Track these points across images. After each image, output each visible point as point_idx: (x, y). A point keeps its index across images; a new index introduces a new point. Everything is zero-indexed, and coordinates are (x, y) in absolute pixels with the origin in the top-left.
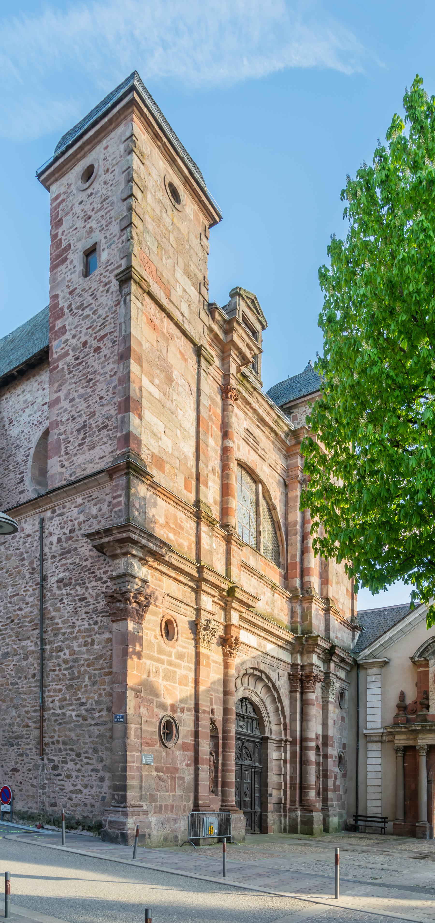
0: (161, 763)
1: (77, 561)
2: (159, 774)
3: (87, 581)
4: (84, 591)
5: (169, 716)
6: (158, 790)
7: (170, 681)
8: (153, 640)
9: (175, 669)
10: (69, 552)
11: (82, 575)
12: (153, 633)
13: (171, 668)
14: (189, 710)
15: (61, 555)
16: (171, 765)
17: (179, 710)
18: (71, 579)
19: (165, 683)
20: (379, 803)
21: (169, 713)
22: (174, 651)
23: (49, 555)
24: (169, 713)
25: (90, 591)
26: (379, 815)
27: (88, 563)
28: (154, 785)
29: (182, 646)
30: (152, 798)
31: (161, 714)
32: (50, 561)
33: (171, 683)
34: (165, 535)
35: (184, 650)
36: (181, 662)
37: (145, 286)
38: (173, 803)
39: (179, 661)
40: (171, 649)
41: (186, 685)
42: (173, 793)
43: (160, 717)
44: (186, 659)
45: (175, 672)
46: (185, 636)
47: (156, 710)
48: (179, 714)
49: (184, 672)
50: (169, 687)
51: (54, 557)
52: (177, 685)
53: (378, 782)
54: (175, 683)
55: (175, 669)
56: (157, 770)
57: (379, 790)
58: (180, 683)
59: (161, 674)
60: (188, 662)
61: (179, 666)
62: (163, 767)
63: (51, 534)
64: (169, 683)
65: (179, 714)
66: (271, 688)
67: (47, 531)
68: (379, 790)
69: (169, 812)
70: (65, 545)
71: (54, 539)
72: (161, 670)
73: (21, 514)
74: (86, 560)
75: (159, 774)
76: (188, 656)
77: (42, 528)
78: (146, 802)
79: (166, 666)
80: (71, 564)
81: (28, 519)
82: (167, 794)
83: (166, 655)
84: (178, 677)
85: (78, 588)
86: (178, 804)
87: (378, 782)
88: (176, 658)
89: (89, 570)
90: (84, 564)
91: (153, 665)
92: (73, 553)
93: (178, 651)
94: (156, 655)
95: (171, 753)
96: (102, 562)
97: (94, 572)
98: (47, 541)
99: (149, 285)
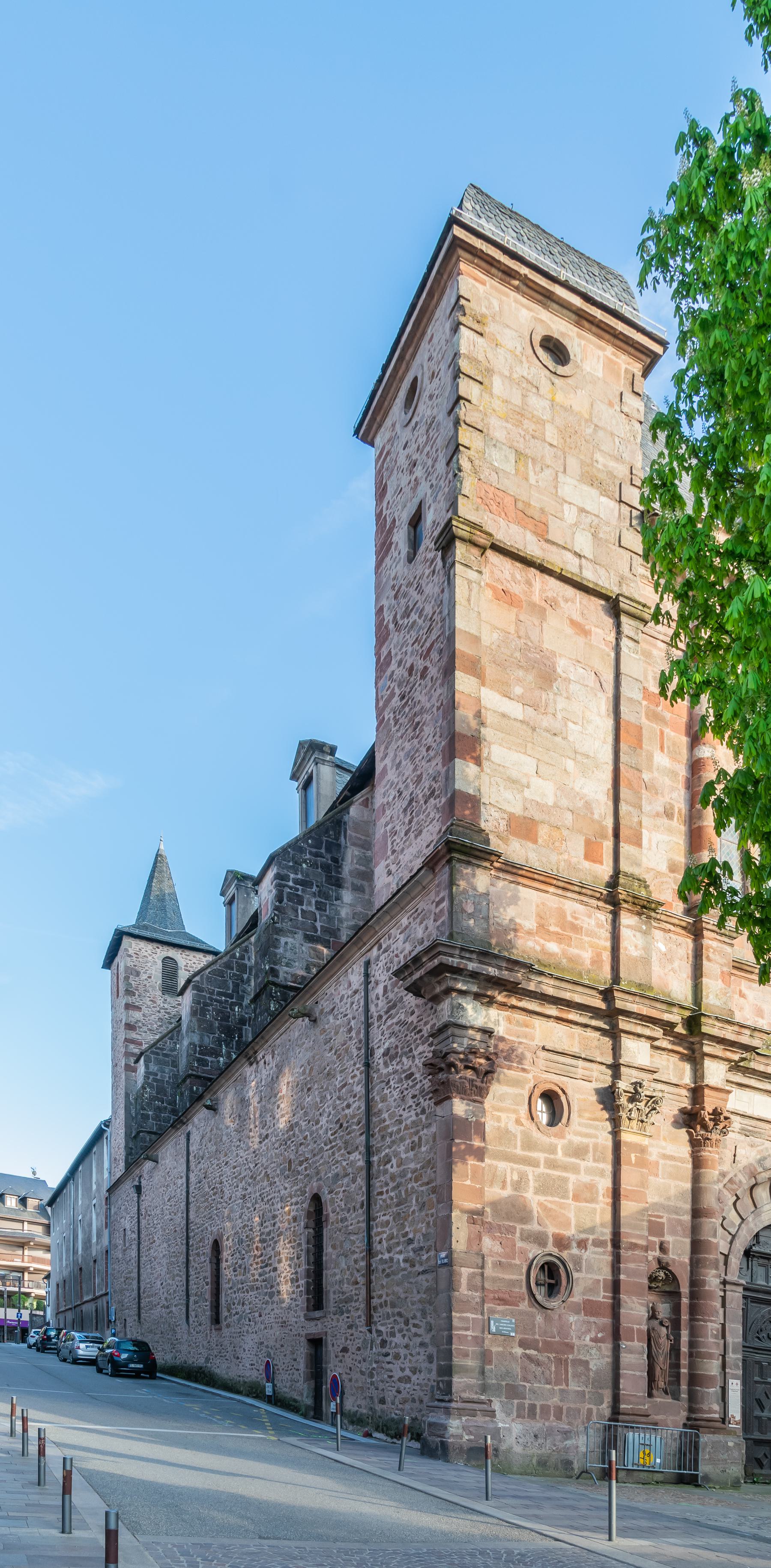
1: (403, 1017)
2: (528, 1352)
3: (413, 1046)
4: (410, 1062)
5: (551, 1255)
6: (525, 1379)
7: (552, 1195)
8: (512, 1127)
10: (394, 1006)
11: (408, 1038)
15: (387, 1012)
18: (397, 1047)
19: (542, 1198)
21: (551, 1248)
23: (375, 1015)
24: (551, 1248)
25: (417, 1061)
27: (413, 1019)
28: (517, 1370)
30: (513, 1392)
31: (533, 1251)
32: (376, 1025)
33: (557, 1199)
37: (482, 540)
43: (531, 1256)
47: (520, 1244)
50: (549, 1205)
51: (380, 1017)
63: (377, 983)
64: (550, 1198)
67: (373, 979)
70: (391, 995)
71: (380, 990)
72: (531, 1177)
73: (347, 961)
74: (413, 1013)
75: (528, 1352)
77: (367, 975)
78: (499, 1396)
79: (542, 1169)
80: (397, 1024)
81: (354, 967)
83: (543, 1150)
85: (404, 1059)
89: (415, 1027)
90: (410, 1020)
91: (512, 1170)
92: (399, 1005)
94: (519, 1151)
96: (429, 1011)
97: (420, 1031)
98: (372, 995)
99: (490, 535)
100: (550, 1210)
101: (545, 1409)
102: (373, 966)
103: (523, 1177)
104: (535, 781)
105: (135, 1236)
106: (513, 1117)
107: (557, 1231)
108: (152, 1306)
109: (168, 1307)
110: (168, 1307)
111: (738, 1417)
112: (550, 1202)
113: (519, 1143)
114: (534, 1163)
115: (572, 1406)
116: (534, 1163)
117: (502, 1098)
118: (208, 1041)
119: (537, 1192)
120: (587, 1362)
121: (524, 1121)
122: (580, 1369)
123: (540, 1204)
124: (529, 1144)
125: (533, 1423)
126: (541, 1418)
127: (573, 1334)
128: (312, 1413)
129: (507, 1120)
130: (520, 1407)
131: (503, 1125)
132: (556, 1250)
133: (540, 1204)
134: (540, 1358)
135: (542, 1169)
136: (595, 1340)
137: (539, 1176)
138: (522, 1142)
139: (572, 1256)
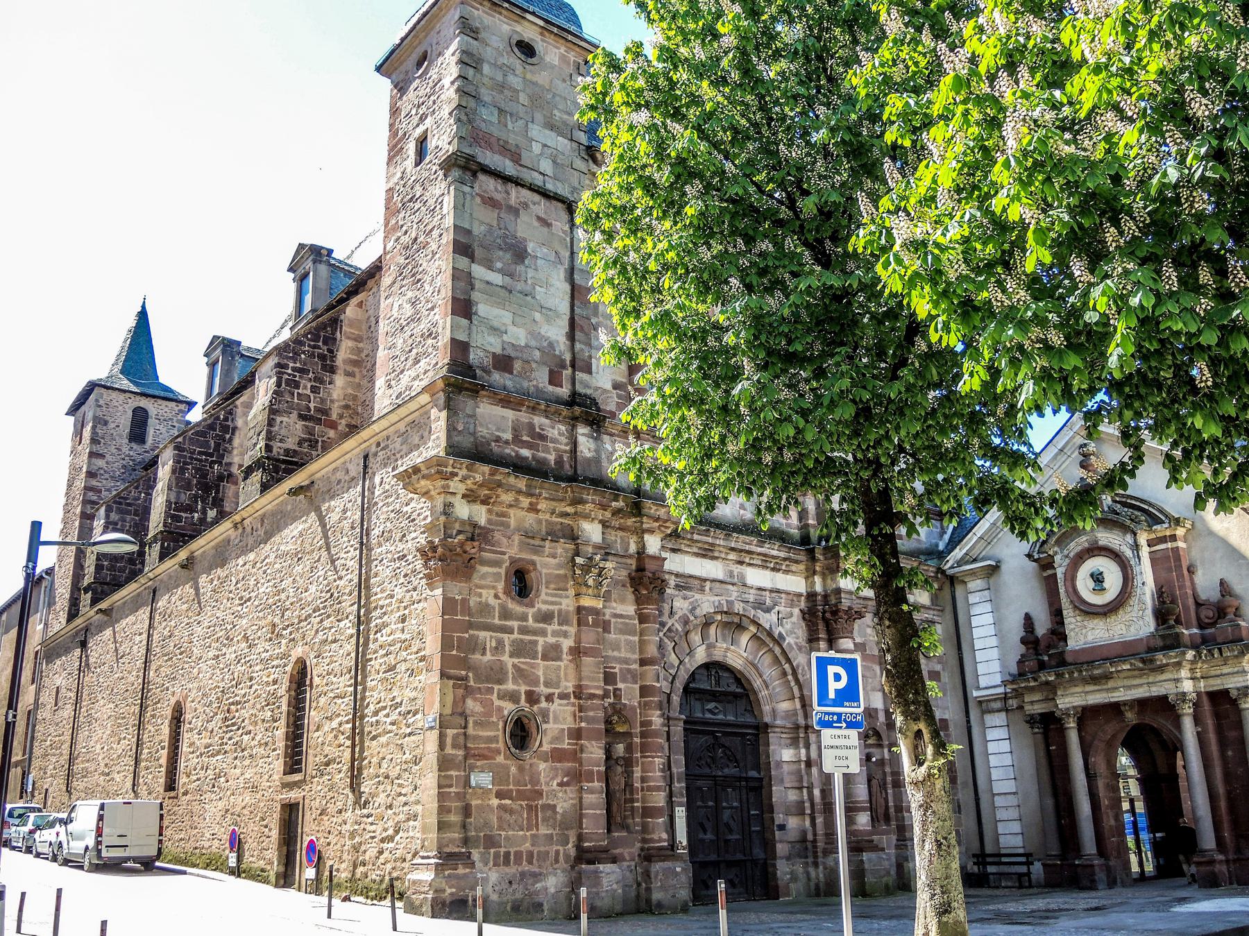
8: (492, 601)
12: (492, 592)
17: (543, 699)
19: (516, 660)
20: (1016, 827)
26: (1021, 851)
35: (551, 607)
45: (536, 642)
49: (551, 640)
50: (523, 666)
53: (1010, 786)
54: (535, 658)
57: (1013, 801)
59: (507, 649)
61: (543, 633)
65: (544, 704)
66: (767, 639)
68: (1013, 801)
84: (540, 649)
87: (1010, 786)
94: (497, 621)
100: (523, 670)
101: (518, 855)
102: (371, 459)
103: (500, 643)
104: (512, 329)
105: (73, 695)
108: (86, 774)
109: (108, 774)
110: (108, 774)
111: (685, 843)
114: (509, 631)
115: (542, 849)
116: (509, 631)
118: (185, 498)
120: (555, 806)
122: (549, 813)
123: (514, 666)
125: (507, 870)
126: (515, 863)
127: (542, 780)
128: (282, 882)
130: (497, 855)
131: (483, 600)
133: (514, 666)
135: (516, 636)
136: (561, 784)
139: (541, 709)
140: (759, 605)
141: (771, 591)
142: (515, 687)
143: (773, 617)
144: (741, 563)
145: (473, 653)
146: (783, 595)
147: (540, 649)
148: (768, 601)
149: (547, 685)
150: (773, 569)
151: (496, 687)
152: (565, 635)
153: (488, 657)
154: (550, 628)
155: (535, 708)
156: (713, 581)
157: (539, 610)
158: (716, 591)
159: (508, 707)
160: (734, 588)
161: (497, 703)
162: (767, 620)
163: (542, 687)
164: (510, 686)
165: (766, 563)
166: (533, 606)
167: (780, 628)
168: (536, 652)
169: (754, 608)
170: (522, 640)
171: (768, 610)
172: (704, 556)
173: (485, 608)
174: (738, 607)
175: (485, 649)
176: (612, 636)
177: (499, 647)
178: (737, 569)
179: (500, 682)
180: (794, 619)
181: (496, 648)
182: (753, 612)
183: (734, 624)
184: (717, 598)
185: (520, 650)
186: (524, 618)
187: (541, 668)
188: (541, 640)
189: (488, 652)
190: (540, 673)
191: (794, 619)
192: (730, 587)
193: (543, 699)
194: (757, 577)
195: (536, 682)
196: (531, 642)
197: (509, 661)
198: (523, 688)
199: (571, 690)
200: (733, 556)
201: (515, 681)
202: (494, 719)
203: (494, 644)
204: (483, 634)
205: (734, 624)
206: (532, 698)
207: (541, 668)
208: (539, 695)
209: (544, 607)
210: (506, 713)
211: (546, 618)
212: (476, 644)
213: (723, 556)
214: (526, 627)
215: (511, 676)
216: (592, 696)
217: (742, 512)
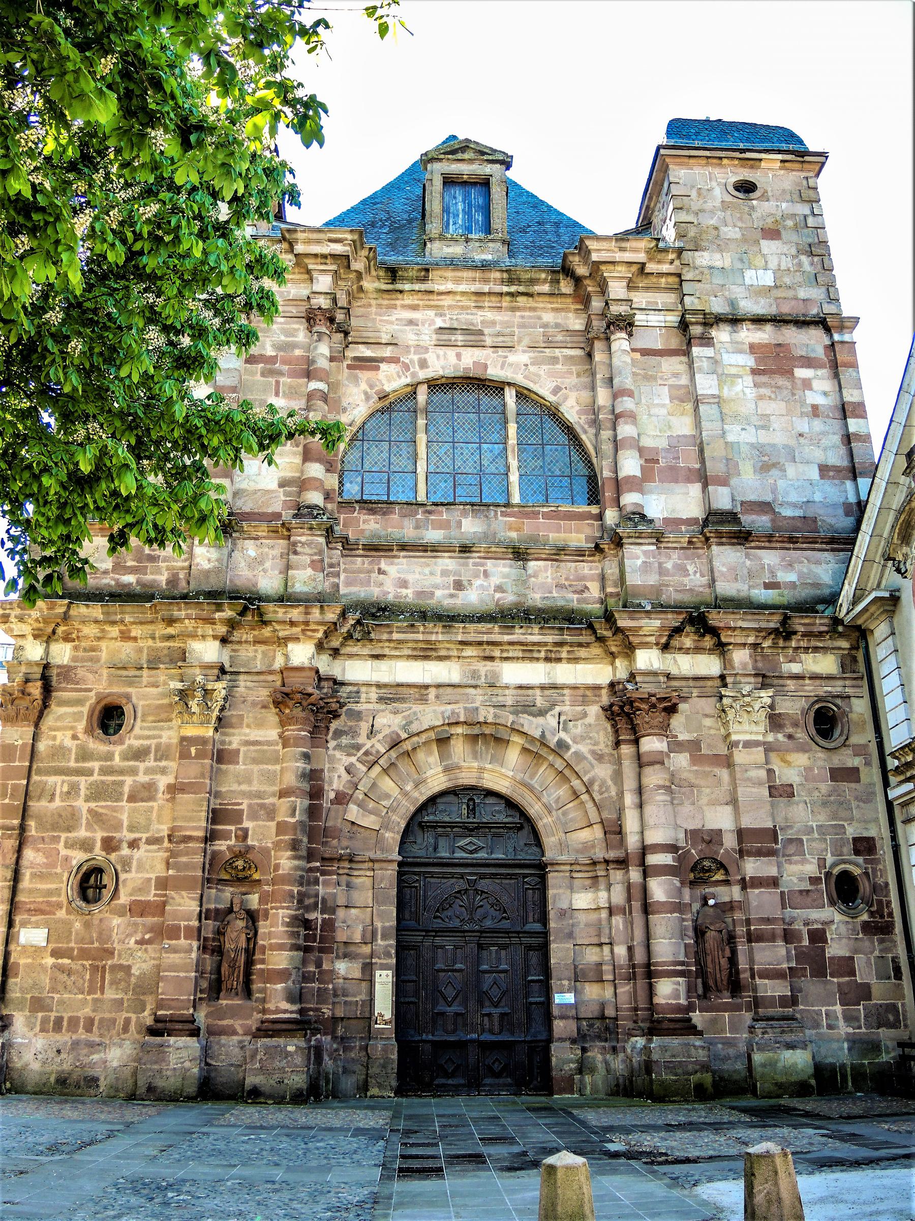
0: (70, 941)
7: (105, 800)
9: (120, 778)
13: (110, 778)
14: (149, 842)
16: (96, 945)
17: (125, 845)
22: (118, 750)
29: (138, 738)
34: (113, 583)
36: (137, 763)
38: (92, 1015)
39: (131, 763)
40: (111, 748)
41: (151, 798)
42: (98, 995)
44: (152, 756)
46: (151, 718)
48: (125, 851)
49: (142, 778)
50: (100, 810)
52: (124, 803)
55: (120, 778)
56: (55, 954)
58: (132, 798)
59: (83, 792)
60: (156, 760)
61: (133, 772)
62: (72, 949)
64: (103, 804)
65: (125, 851)
69: (81, 1030)
76: (156, 751)
82: (80, 996)
84: (126, 789)
86: (107, 1015)
88: (125, 757)
93: (130, 746)
95: (96, 922)
100: (101, 814)
106: (69, 733)
107: (105, 835)
112: (102, 807)
113: (73, 757)
114: (89, 773)
116: (89, 773)
117: (60, 718)
119: (87, 800)
121: (80, 735)
123: (90, 811)
124: (84, 755)
129: (64, 738)
132: (104, 853)
133: (90, 811)
134: (74, 967)
135: (96, 777)
137: (91, 784)
138: (77, 754)
140: (528, 708)
141: (543, 688)
142: (88, 834)
143: (551, 720)
144: (491, 658)
145: (39, 799)
146: (566, 692)
147: (126, 789)
148: (540, 702)
149: (131, 829)
150: (547, 659)
151: (64, 836)
152: (164, 771)
153: (58, 803)
154: (142, 766)
155: (113, 857)
156: (438, 686)
157: (130, 746)
158: (446, 698)
159: (78, 857)
160: (479, 691)
161: (64, 852)
162: (532, 725)
163: (125, 832)
164: (82, 833)
165: (529, 653)
166: (122, 743)
167: (563, 735)
168: (121, 794)
169: (516, 713)
170: (103, 782)
171: (542, 713)
172: (426, 658)
173: (59, 751)
174: (487, 714)
175: (53, 795)
176: (241, 767)
177: (73, 790)
178: (484, 668)
179: (69, 829)
180: (591, 719)
181: (69, 793)
182: (511, 718)
183: (488, 737)
184: (449, 707)
185: (97, 793)
186: (109, 757)
187: (125, 811)
188: (129, 781)
189: (57, 798)
190: (125, 817)
191: (591, 719)
192: (472, 691)
193: (125, 845)
194: (515, 673)
195: (118, 827)
196: (114, 783)
197: (82, 805)
198: (99, 835)
199: (165, 833)
200: (469, 652)
201: (89, 827)
202: (59, 870)
203: (65, 789)
204: (51, 779)
205: (488, 737)
206: (109, 845)
207: (125, 811)
208: (121, 841)
209: (137, 743)
210: (74, 862)
211: (140, 754)
212: (43, 790)
213: (455, 653)
214: (112, 767)
215: (84, 822)
216: (189, 839)
217: (498, 595)
